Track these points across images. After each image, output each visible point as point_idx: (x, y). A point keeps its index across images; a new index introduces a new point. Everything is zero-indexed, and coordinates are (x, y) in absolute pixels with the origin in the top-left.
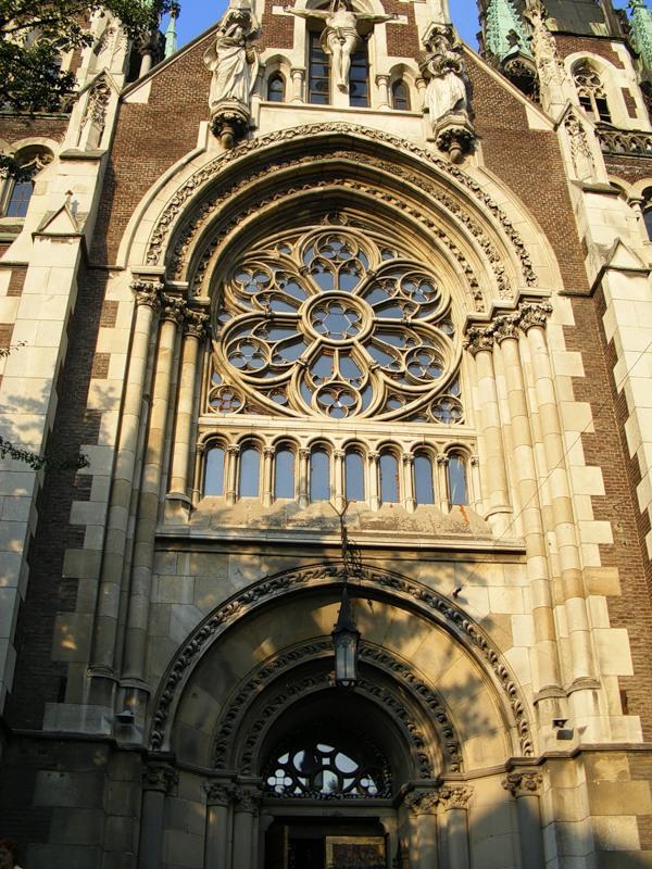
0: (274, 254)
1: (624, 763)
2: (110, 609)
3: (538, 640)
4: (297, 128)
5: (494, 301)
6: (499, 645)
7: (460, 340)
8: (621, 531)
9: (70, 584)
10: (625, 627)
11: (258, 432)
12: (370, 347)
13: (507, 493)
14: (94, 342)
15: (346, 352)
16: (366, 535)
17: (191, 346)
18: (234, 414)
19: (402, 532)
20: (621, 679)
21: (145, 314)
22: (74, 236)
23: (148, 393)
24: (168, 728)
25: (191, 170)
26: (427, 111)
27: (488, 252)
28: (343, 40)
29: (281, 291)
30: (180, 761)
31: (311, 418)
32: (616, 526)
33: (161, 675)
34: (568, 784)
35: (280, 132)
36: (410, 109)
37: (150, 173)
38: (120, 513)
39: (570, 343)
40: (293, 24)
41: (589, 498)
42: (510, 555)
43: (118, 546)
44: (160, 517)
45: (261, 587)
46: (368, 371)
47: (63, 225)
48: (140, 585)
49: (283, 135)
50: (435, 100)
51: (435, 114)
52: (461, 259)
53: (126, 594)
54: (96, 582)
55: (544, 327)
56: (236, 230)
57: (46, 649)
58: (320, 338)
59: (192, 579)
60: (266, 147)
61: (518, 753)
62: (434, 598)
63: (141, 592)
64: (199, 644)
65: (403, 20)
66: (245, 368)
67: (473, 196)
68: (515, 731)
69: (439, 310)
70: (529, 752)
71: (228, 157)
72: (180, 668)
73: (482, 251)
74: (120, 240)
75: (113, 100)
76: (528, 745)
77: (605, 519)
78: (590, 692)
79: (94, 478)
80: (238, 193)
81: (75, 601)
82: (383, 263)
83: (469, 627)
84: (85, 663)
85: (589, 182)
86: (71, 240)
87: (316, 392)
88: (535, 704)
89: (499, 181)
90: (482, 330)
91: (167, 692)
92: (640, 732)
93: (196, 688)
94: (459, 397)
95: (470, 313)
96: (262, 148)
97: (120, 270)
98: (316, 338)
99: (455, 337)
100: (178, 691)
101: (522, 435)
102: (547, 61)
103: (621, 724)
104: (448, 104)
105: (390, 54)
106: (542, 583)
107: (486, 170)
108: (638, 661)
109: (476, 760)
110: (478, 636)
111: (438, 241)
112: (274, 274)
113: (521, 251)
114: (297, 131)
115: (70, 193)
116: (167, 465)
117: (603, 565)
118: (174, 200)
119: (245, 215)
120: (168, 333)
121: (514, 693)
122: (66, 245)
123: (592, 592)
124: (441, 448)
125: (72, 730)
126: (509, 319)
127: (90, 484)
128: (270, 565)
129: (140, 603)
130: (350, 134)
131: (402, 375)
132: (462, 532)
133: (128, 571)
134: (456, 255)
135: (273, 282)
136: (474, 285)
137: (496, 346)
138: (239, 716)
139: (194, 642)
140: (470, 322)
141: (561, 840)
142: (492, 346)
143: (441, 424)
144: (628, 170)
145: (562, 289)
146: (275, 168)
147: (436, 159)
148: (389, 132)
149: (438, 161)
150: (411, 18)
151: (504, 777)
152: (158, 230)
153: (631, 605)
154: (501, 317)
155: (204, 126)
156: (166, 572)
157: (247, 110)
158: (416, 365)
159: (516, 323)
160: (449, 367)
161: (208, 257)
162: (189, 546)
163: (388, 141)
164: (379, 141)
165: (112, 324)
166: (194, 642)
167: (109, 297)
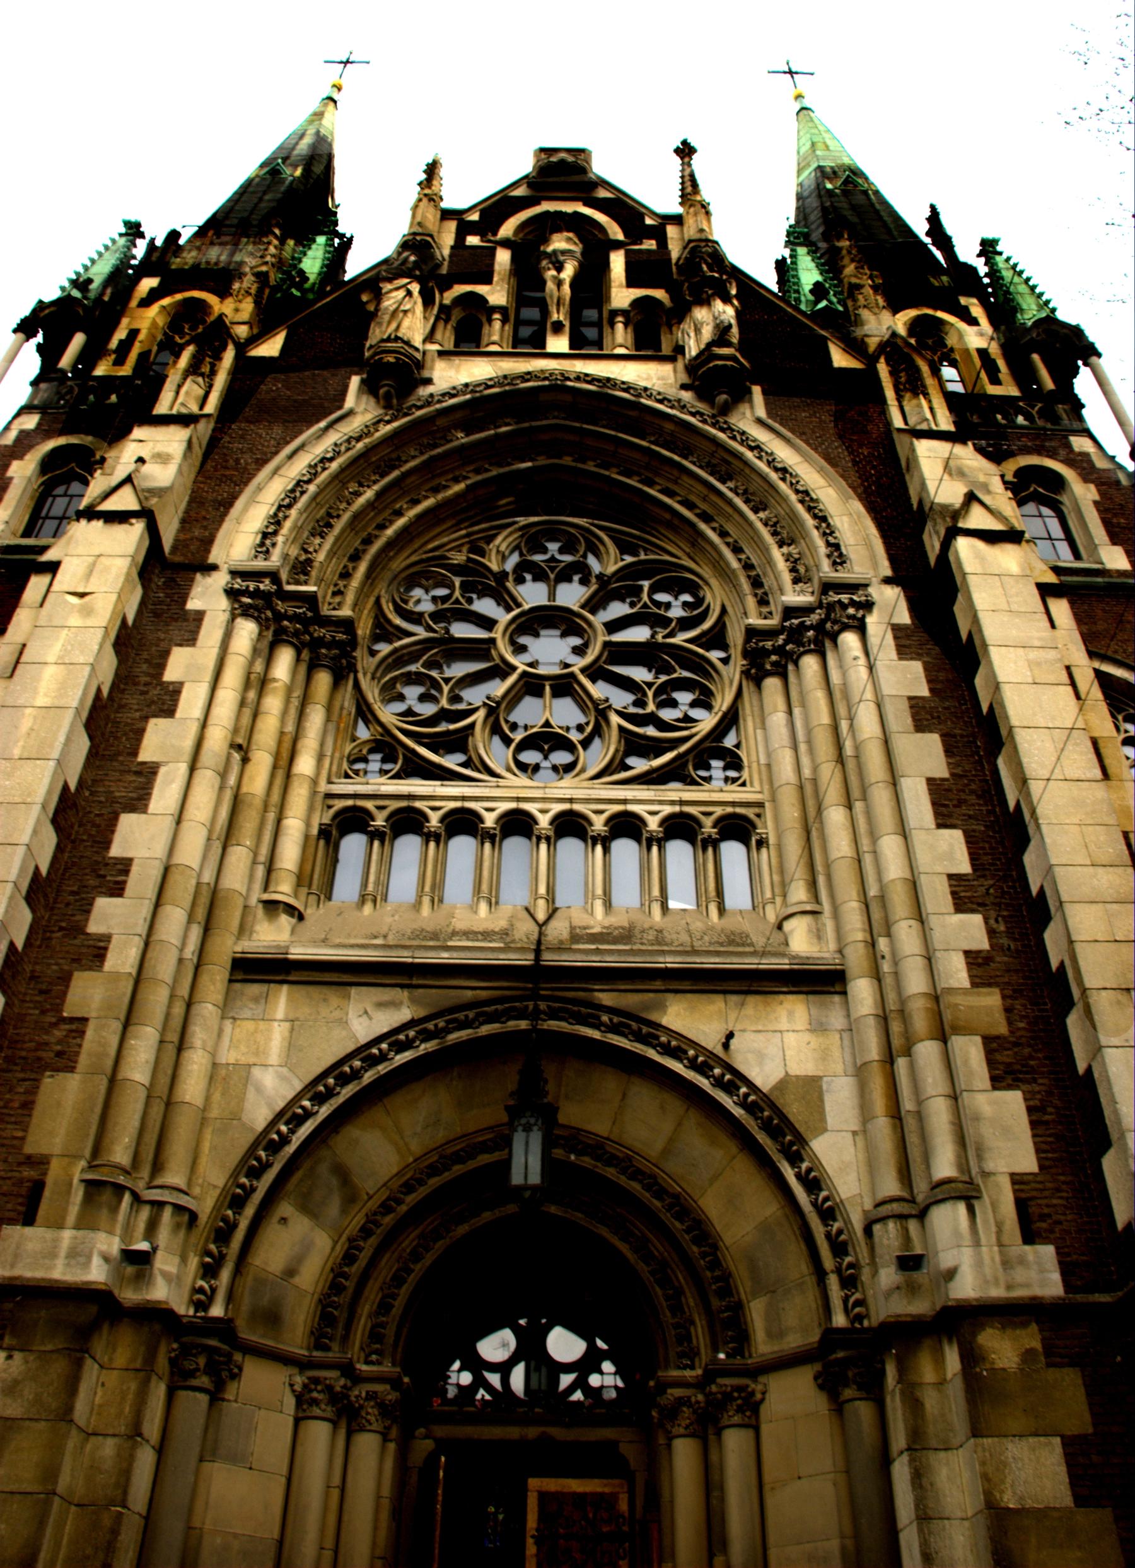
0: (459, 558)
1: (1030, 1337)
3: (866, 1114)
4: (491, 379)
5: (784, 598)
6: (802, 1129)
7: (738, 663)
8: (1002, 928)
9: (74, 1027)
10: (1016, 1088)
11: (418, 804)
12: (601, 684)
13: (813, 885)
14: (162, 667)
15: (564, 686)
17: (323, 679)
18: (383, 780)
19: (637, 947)
20: (1017, 1179)
21: (247, 629)
23: (240, 741)
24: (225, 1275)
25: (333, 437)
26: (680, 350)
27: (774, 534)
28: (560, 268)
29: (467, 606)
31: (502, 782)
32: (992, 922)
33: (221, 1183)
34: (928, 1374)
35: (466, 385)
36: (660, 351)
37: (272, 442)
38: (174, 918)
39: (904, 651)
41: (945, 878)
43: (164, 967)
44: (243, 930)
45: (402, 1037)
46: (593, 713)
47: (125, 501)
48: (199, 1035)
49: (471, 388)
50: (692, 334)
51: (693, 349)
52: (737, 550)
53: (171, 1050)
54: (117, 1026)
55: (861, 628)
56: (401, 522)
57: (20, 1134)
58: (522, 668)
59: (287, 1025)
60: (444, 405)
61: (840, 1320)
62: (691, 1053)
63: (198, 1043)
64: (292, 1131)
65: (650, 245)
66: (409, 712)
67: (749, 455)
68: (833, 1281)
69: (707, 625)
70: (859, 1318)
71: (387, 418)
72: (256, 1173)
73: (765, 532)
74: (217, 529)
75: (229, 356)
76: (859, 1303)
77: (973, 911)
78: (961, 1208)
79: (135, 862)
80: (403, 469)
81: (77, 1054)
82: (621, 564)
83: (752, 1098)
84: (80, 1157)
85: (924, 426)
86: (133, 521)
87: (513, 746)
88: (868, 1231)
89: (789, 434)
90: (769, 644)
91: (230, 1212)
92: (1056, 1276)
93: (285, 1208)
94: (738, 746)
95: (751, 621)
96: (438, 406)
97: (214, 568)
98: (514, 668)
99: (732, 662)
100: (250, 1211)
101: (832, 793)
102: (859, 287)
103: (1022, 1261)
104: (707, 333)
105: (631, 282)
106: (871, 1021)
107: (770, 422)
108: (1044, 1147)
109: (770, 1335)
110: (766, 1113)
111: (703, 526)
112: (457, 584)
113: (824, 525)
114: (490, 383)
115: (141, 460)
116: (264, 851)
117: (974, 985)
118: (304, 475)
119: (415, 502)
120: (284, 660)
121: (831, 1209)
122: (124, 527)
123: (958, 1030)
124: (708, 822)
125: (39, 1274)
126: (808, 623)
127: (126, 872)
128: (413, 1000)
129: (196, 1063)
130: (569, 383)
131: (652, 719)
132: (738, 945)
133: (178, 1010)
134: (728, 544)
135: (457, 594)
136: (756, 583)
137: (791, 667)
138: (364, 1257)
139: (284, 1128)
140: (751, 633)
141: (921, 1486)
142: (785, 667)
143: (707, 786)
144: (989, 445)
145: (888, 572)
146: (460, 435)
147: (693, 410)
148: (624, 379)
149: (698, 413)
151: (818, 1367)
152: (275, 515)
153: (1027, 1051)
154: (796, 622)
155: (355, 381)
156: (247, 1013)
157: (419, 356)
158: (674, 704)
159: (819, 627)
160: (723, 702)
161: (355, 557)
162: (288, 973)
163: (626, 390)
164: (610, 391)
166: (284, 1128)
167: (193, 604)
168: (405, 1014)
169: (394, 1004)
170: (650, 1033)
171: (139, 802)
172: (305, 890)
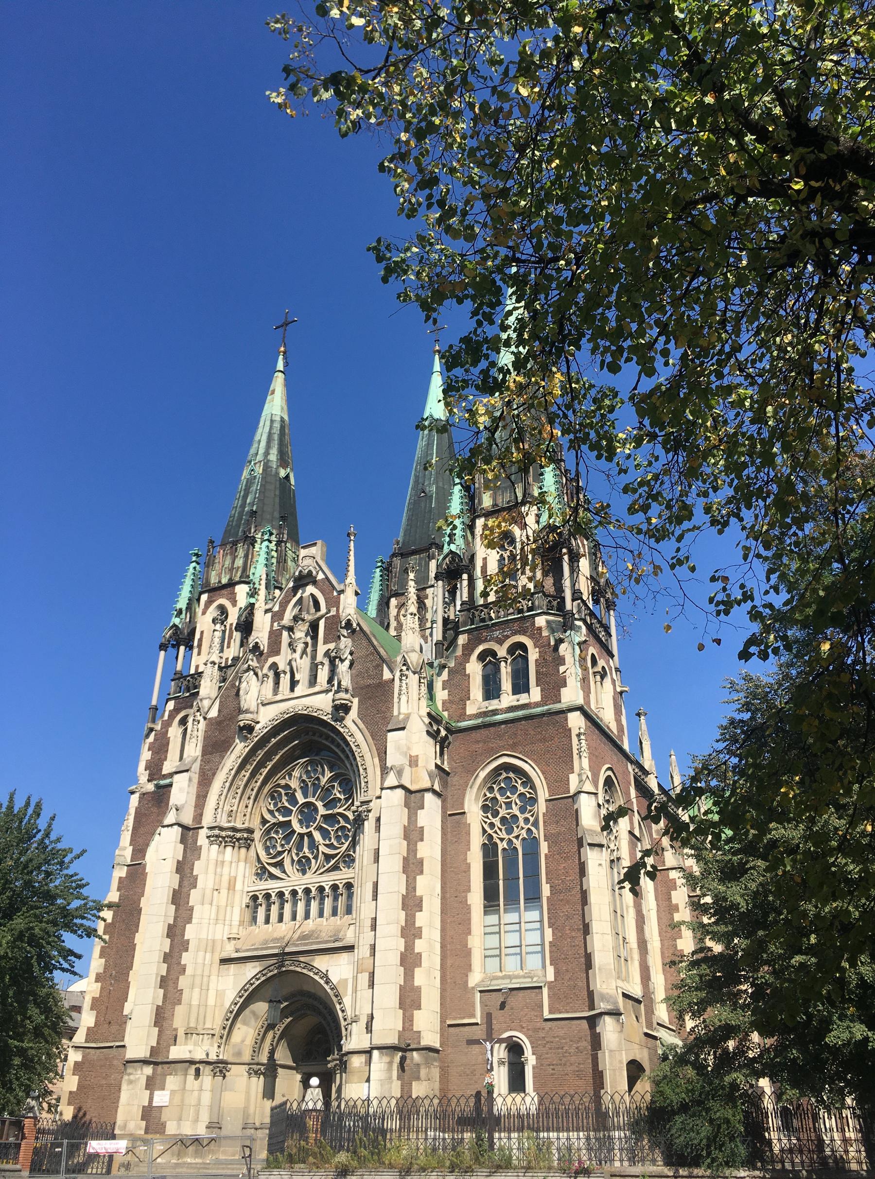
0: (283, 782)
2: (195, 1002)
11: (269, 891)
16: (297, 945)
17: (243, 850)
22: (175, 824)
25: (233, 757)
30: (230, 1060)
40: (281, 635)
42: (350, 948)
48: (212, 986)
65: (333, 612)
67: (349, 739)
89: (362, 726)
93: (238, 1025)
97: (202, 827)
100: (227, 1030)
111: (346, 762)
129: (212, 994)
150: (338, 610)
165: (199, 858)
168: (258, 969)
169: (255, 967)
170: (311, 968)
171: (189, 920)
172: (241, 928)
